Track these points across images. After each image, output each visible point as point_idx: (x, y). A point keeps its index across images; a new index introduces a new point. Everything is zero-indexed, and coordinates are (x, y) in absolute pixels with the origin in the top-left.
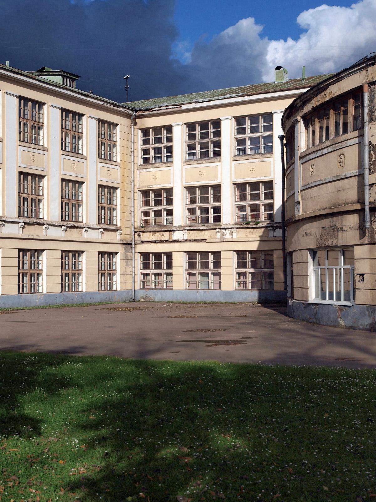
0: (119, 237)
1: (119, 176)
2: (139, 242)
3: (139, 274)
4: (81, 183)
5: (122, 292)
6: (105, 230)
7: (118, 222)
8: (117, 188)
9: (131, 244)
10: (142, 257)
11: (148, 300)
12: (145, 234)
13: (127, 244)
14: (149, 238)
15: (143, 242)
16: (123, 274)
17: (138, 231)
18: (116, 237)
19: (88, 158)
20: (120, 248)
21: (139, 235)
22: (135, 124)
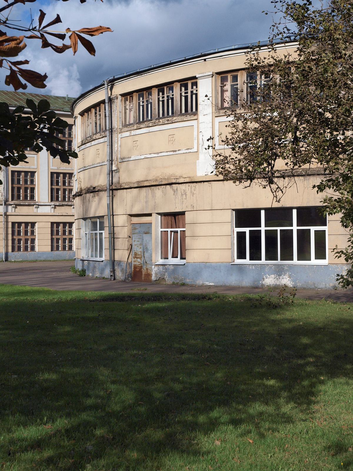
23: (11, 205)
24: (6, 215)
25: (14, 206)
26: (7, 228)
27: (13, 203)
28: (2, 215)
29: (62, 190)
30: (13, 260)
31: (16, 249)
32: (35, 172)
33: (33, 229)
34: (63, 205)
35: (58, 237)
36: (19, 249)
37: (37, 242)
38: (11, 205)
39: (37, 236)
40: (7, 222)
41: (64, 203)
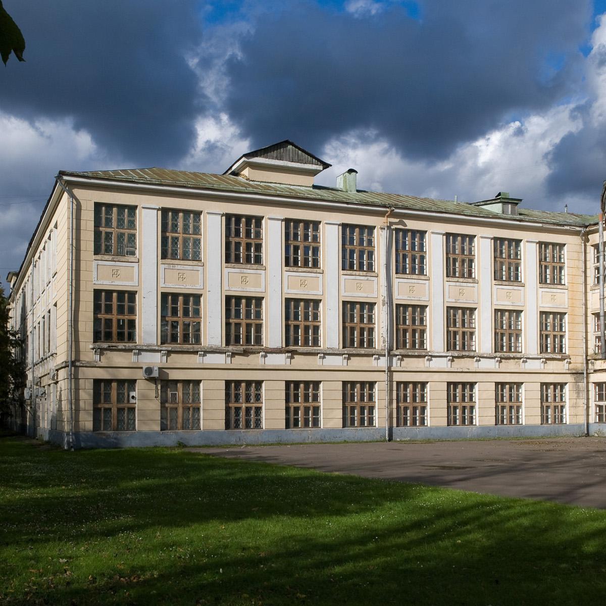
0: (567, 366)
1: (566, 300)
2: (592, 371)
3: (594, 405)
4: (519, 312)
5: (572, 426)
6: (547, 359)
7: (567, 350)
8: (565, 313)
9: (583, 373)
10: (597, 387)
11: (600, 435)
12: (597, 362)
13: (577, 373)
14: (601, 366)
15: (595, 371)
16: (574, 406)
17: (591, 358)
18: (563, 366)
19: (527, 285)
20: (568, 378)
21: (593, 363)
22: (588, 240)
23: (397, 355)
24: (390, 372)
25: (400, 357)
26: (391, 390)
27: (398, 354)
28: (385, 371)
29: (460, 333)
30: (398, 440)
31: (349, 422)
32: (426, 306)
33: (423, 393)
34: (463, 357)
35: (455, 404)
36: (405, 424)
37: (428, 412)
38: (397, 355)
39: (428, 404)
40: (391, 381)
41: (464, 353)
